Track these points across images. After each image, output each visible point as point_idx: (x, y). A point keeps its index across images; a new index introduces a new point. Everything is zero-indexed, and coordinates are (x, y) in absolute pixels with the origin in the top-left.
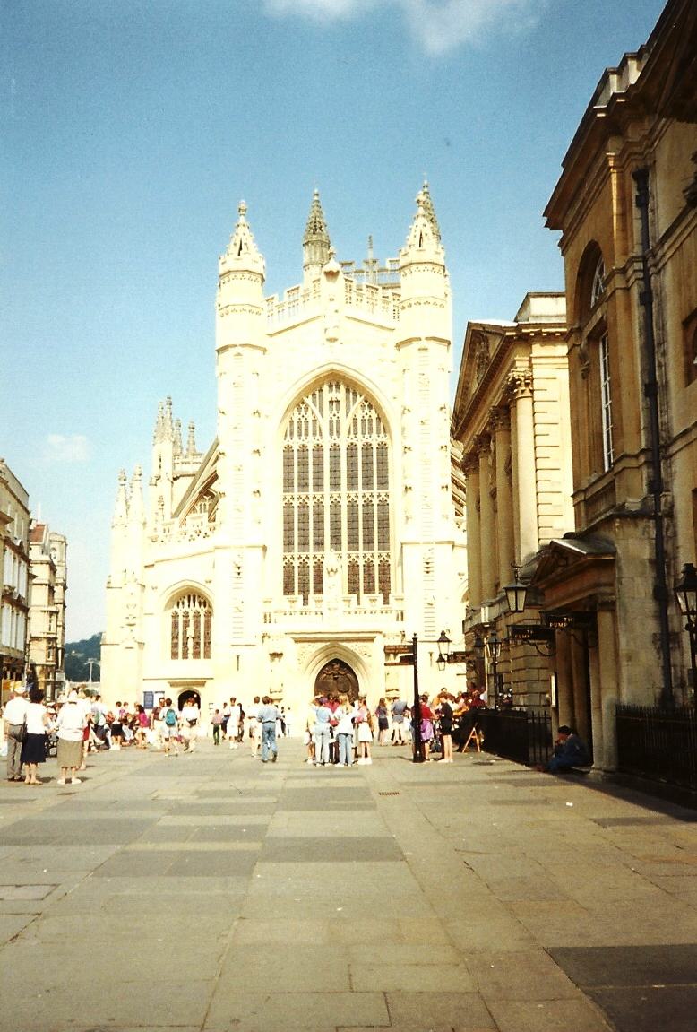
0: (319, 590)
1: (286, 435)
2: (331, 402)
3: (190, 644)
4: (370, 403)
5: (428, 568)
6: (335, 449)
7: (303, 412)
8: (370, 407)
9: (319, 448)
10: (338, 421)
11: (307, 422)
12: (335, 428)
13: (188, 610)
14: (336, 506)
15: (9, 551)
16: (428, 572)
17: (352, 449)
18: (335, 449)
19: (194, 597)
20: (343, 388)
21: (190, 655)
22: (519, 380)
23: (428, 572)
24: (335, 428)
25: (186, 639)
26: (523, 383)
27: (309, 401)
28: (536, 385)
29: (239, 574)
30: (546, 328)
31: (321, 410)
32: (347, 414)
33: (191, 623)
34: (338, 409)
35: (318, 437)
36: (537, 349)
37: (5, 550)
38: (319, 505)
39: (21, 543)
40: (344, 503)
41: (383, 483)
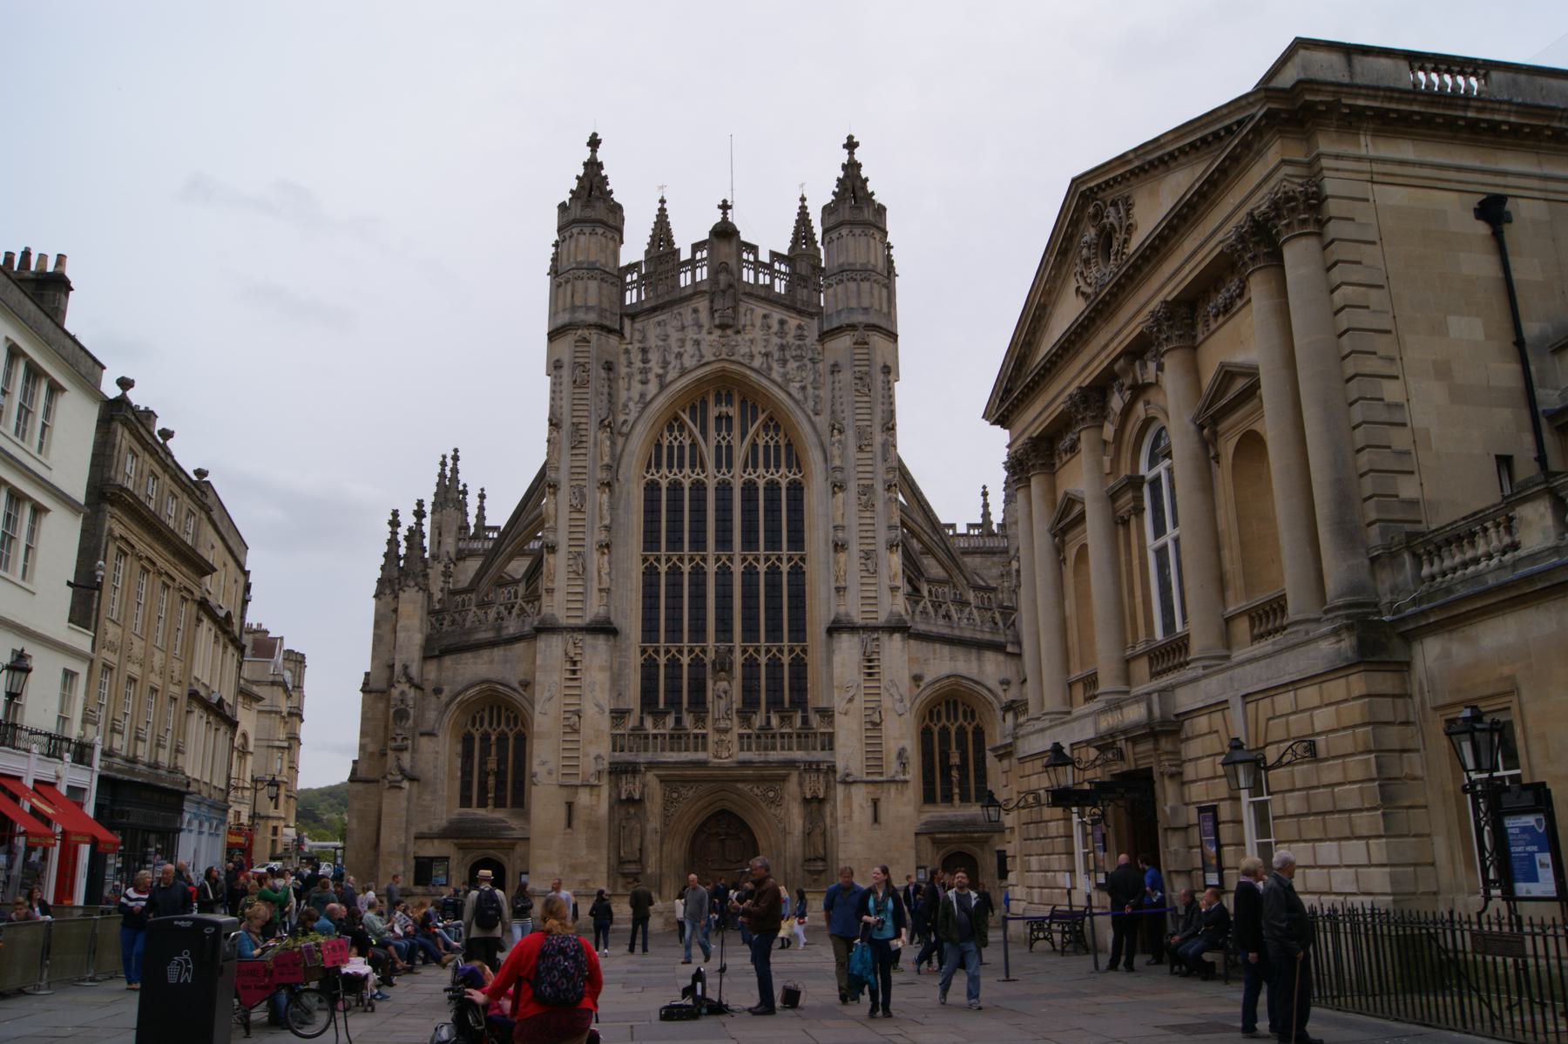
0: (699, 703)
1: (649, 466)
2: (719, 418)
3: (491, 781)
4: (775, 423)
5: (870, 667)
6: (724, 489)
7: (676, 433)
8: (777, 428)
9: (698, 487)
10: (729, 447)
11: (681, 448)
12: (724, 457)
13: (490, 730)
14: (724, 574)
15: (206, 623)
16: (870, 674)
17: (749, 488)
18: (724, 489)
19: (499, 708)
20: (736, 399)
21: (490, 802)
22: (1289, 199)
23: (870, 674)
24: (724, 457)
25: (484, 774)
26: (1301, 207)
27: (686, 417)
28: (1332, 207)
29: (574, 672)
30: (1349, 95)
31: (704, 431)
32: (743, 435)
33: (494, 749)
34: (729, 429)
35: (698, 470)
36: (1326, 144)
37: (199, 620)
38: (698, 574)
39: (228, 614)
40: (737, 569)
41: (797, 540)
